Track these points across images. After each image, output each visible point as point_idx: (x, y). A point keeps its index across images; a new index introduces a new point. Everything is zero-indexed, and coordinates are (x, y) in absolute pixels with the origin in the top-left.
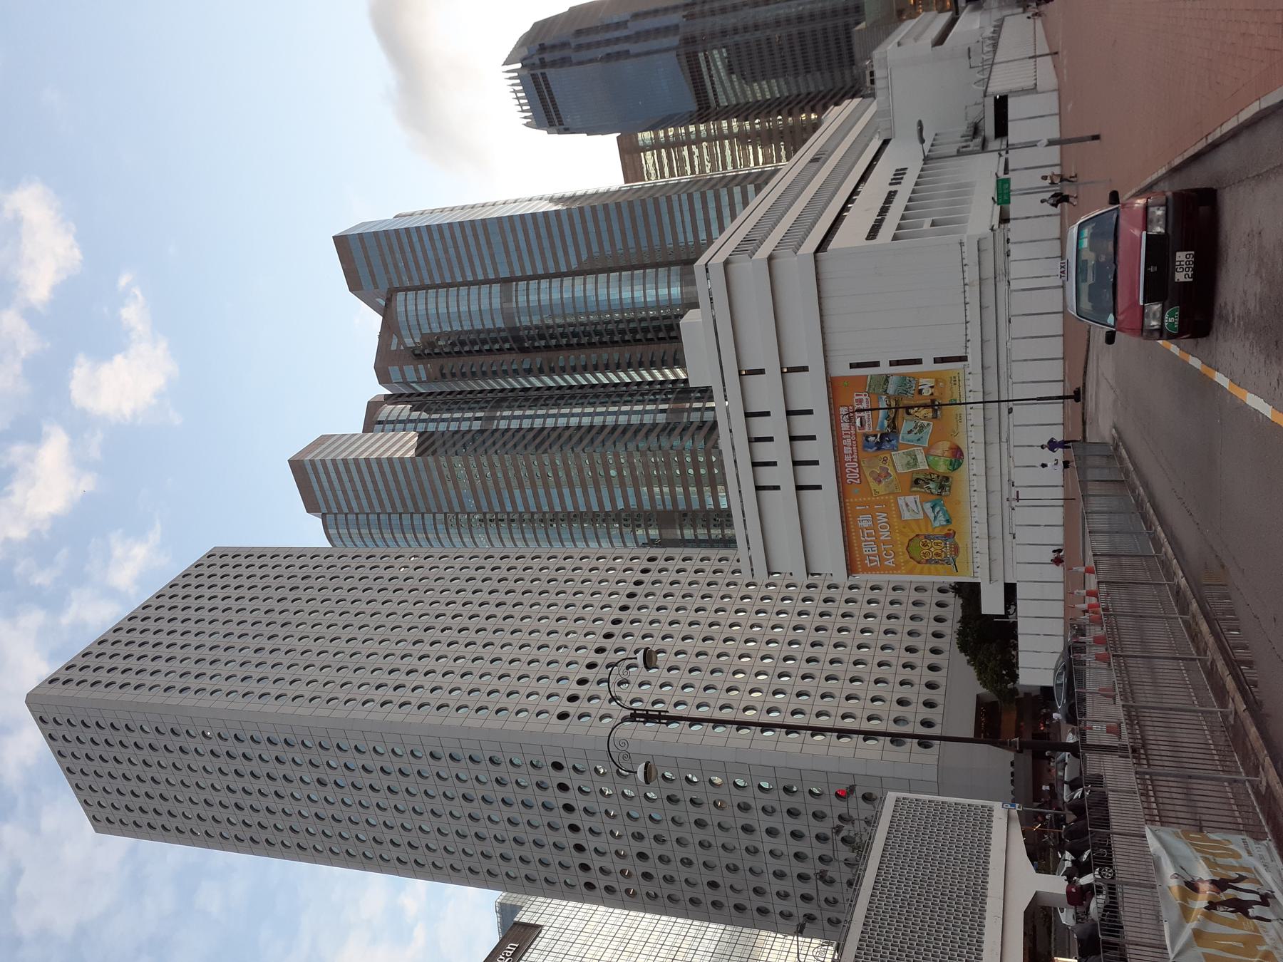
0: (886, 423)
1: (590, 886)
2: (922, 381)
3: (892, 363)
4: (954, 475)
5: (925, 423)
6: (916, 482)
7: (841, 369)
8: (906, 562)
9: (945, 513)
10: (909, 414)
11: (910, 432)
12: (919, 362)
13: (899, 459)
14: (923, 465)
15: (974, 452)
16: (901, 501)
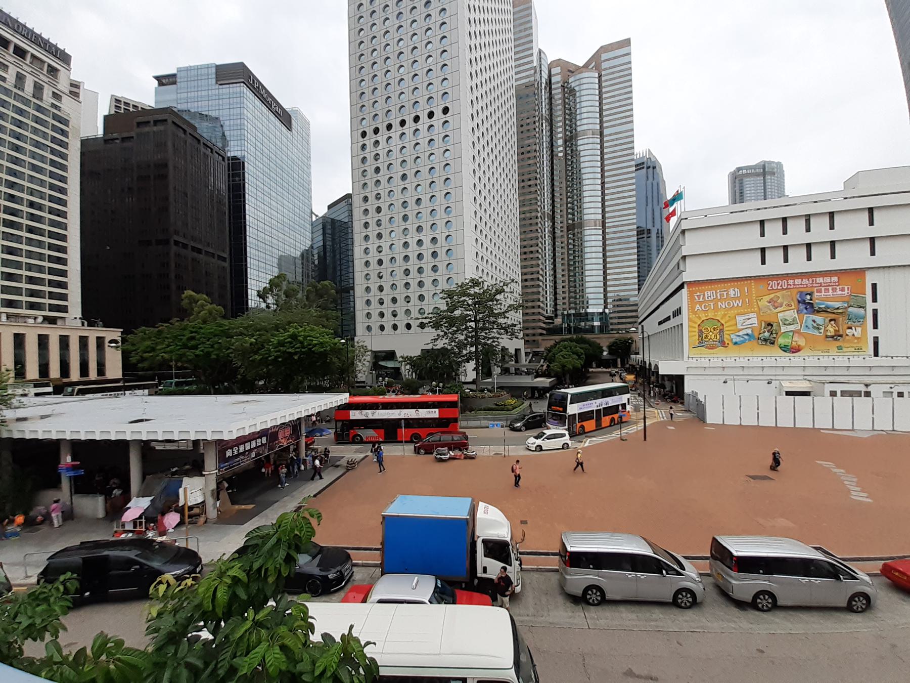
0: (823, 306)
1: (364, 134)
2: (859, 329)
3: (875, 313)
4: (776, 347)
5: (822, 331)
6: (770, 325)
7: (870, 279)
8: (700, 318)
9: (743, 342)
10: (831, 320)
11: (814, 321)
12: (875, 326)
13: (791, 314)
14: (784, 329)
15: (796, 360)
16: (751, 315)
